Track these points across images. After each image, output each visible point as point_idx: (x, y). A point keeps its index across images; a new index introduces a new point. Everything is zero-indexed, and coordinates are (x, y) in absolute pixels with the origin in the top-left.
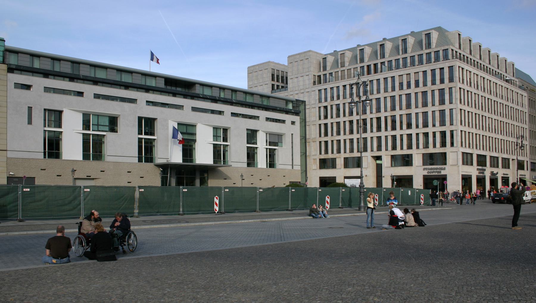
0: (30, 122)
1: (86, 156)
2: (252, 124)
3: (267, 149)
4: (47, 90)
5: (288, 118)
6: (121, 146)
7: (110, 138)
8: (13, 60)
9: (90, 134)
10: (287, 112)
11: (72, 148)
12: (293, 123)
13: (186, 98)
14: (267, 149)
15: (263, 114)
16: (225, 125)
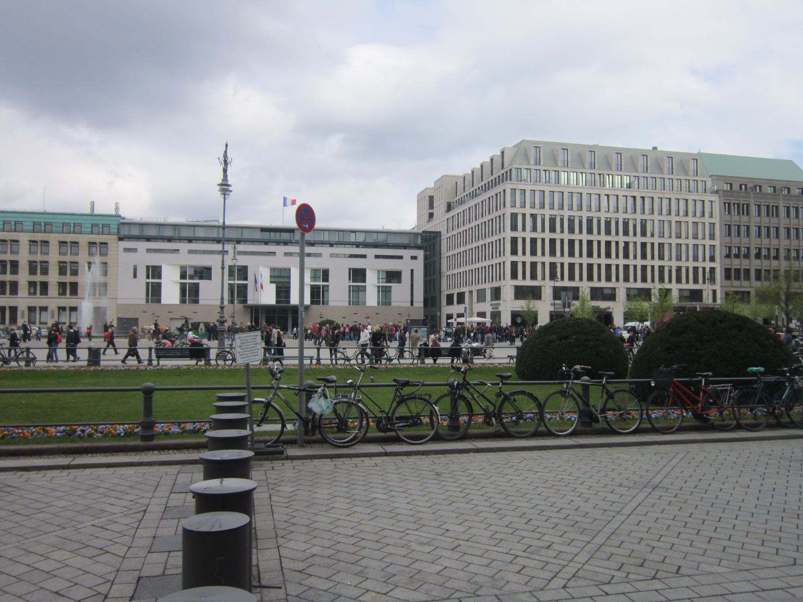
0: (135, 276)
1: (183, 301)
2: (358, 264)
3: (379, 287)
4: (149, 250)
5: (407, 253)
6: (212, 292)
7: (203, 284)
8: (125, 231)
9: (186, 283)
10: (405, 247)
11: (171, 294)
12: (414, 258)
13: (279, 245)
14: (379, 287)
15: (371, 252)
16: (325, 267)
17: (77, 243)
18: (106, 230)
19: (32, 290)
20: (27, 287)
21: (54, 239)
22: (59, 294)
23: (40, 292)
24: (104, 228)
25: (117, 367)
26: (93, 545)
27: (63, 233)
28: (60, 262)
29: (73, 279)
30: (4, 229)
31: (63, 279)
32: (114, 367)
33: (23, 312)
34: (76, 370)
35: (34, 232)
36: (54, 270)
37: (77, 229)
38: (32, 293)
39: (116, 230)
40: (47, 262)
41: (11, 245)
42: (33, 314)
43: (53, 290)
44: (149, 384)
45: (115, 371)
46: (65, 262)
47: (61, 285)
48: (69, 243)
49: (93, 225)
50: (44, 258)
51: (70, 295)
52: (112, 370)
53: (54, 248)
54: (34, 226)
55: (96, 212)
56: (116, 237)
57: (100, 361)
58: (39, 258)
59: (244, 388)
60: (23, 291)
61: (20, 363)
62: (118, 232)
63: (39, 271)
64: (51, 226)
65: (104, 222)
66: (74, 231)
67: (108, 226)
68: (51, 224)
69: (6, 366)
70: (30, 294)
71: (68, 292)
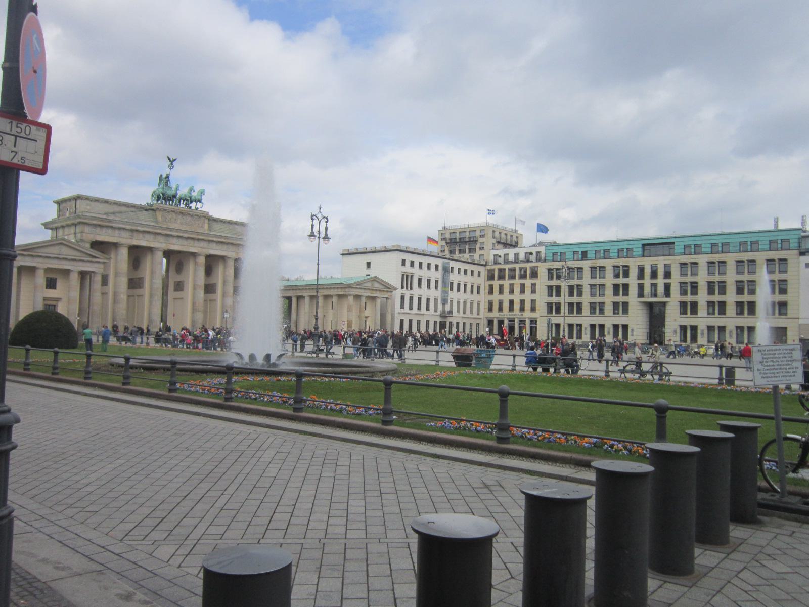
17: (754, 261)
18: (785, 245)
19: (711, 310)
20: (706, 307)
21: (731, 259)
22: (737, 314)
23: (719, 311)
24: (753, 245)
25: (748, 388)
26: (762, 580)
27: (740, 252)
28: (737, 282)
29: (750, 298)
30: (684, 253)
31: (741, 298)
32: (745, 387)
33: (702, 331)
34: (705, 388)
35: (712, 253)
36: (731, 290)
37: (755, 248)
38: (711, 313)
39: (796, 245)
40: (724, 282)
41: (719, 266)
42: (712, 333)
43: (731, 310)
44: (662, 401)
45: (745, 392)
46: (742, 282)
47: (682, 304)
48: (777, 261)
49: (741, 243)
50: (722, 278)
51: (719, 314)
52: (741, 390)
53: (731, 268)
54: (712, 248)
55: (781, 227)
56: (796, 252)
57: (734, 380)
58: (717, 278)
59: (772, 418)
60: (702, 310)
61: (655, 377)
62: (800, 247)
63: (717, 291)
64: (757, 245)
65: (783, 238)
66: (782, 248)
67: (788, 241)
68: (728, 244)
69: (643, 379)
70: (709, 314)
71: (746, 311)
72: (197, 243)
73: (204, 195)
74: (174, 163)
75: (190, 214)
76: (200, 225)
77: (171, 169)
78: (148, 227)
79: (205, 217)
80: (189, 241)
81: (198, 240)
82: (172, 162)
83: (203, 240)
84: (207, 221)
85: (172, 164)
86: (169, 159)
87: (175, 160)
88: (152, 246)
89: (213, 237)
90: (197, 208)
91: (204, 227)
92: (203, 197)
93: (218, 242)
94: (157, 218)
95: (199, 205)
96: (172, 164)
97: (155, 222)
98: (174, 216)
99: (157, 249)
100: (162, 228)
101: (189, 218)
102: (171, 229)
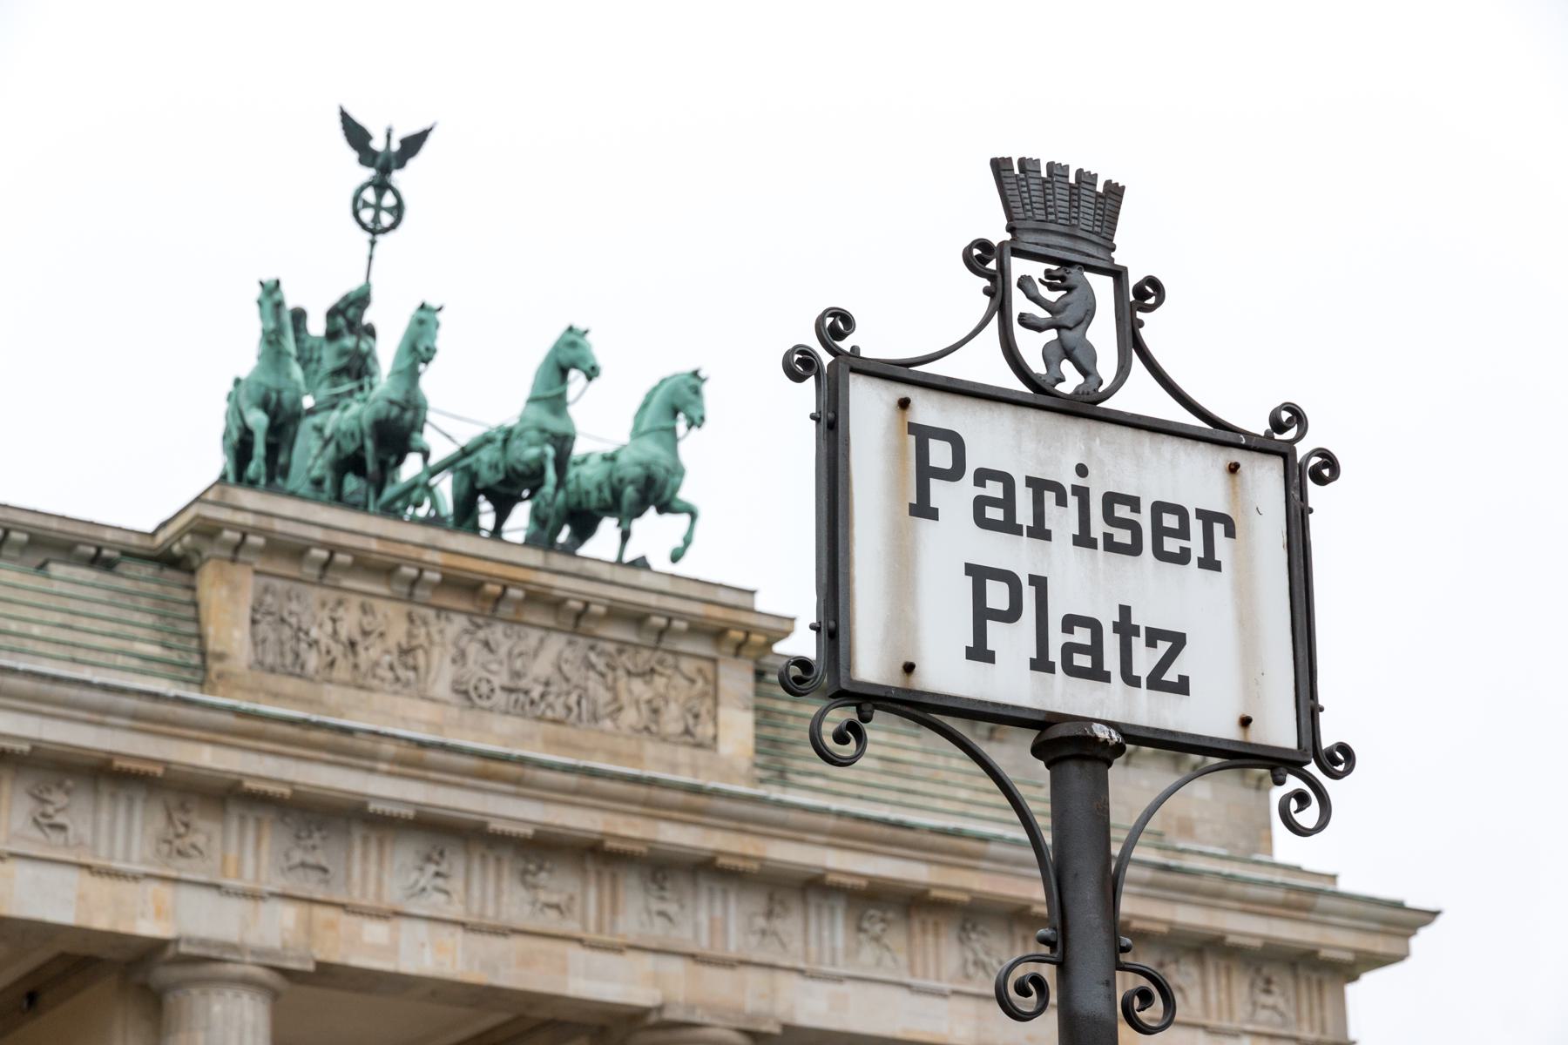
72: (636, 910)
73: (695, 422)
74: (398, 178)
75: (557, 605)
76: (672, 721)
77: (375, 230)
78: (100, 716)
79: (718, 634)
80: (559, 884)
81: (663, 869)
82: (383, 161)
83: (707, 870)
84: (736, 679)
85: (381, 186)
86: (356, 135)
87: (413, 145)
88: (148, 927)
89: (798, 834)
90: (641, 564)
91: (711, 744)
92: (692, 447)
93: (873, 901)
94: (200, 637)
95: (653, 534)
96: (381, 186)
97: (175, 669)
98: (392, 618)
99: (202, 964)
100: (251, 729)
101: (548, 655)
102: (343, 744)
